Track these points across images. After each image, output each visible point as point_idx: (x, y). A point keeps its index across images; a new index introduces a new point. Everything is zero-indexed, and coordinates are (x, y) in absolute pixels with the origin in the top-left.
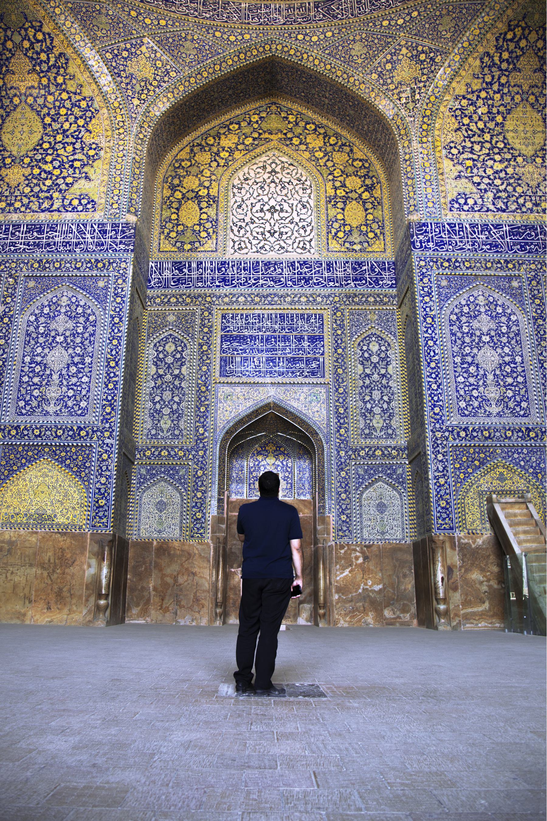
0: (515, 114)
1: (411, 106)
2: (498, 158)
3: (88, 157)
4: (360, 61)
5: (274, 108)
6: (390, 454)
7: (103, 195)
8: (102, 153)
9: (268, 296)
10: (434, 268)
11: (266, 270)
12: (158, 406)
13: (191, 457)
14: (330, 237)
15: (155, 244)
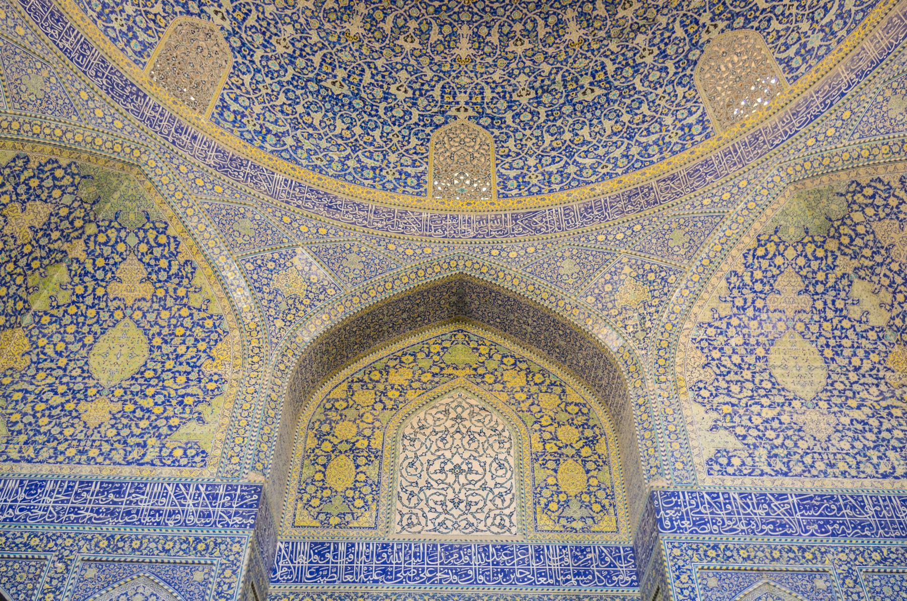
0: (780, 345)
1: (641, 335)
2: (765, 401)
3: (206, 392)
4: (571, 281)
5: (460, 336)
7: (219, 444)
8: (226, 387)
10: (695, 559)
11: (447, 558)
14: (539, 509)
15: (289, 516)
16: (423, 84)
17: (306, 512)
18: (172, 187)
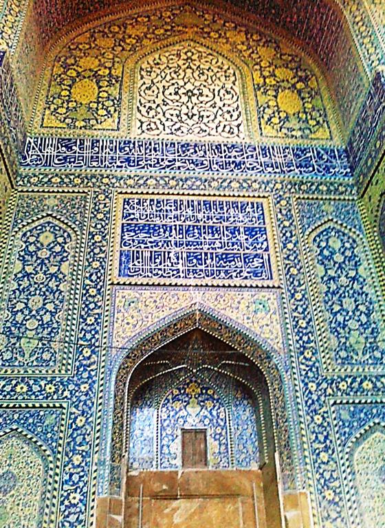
5: (187, 7)
9: (187, 179)
11: (184, 152)
12: (19, 317)
13: (66, 393)
15: (38, 119)
17: (53, 117)
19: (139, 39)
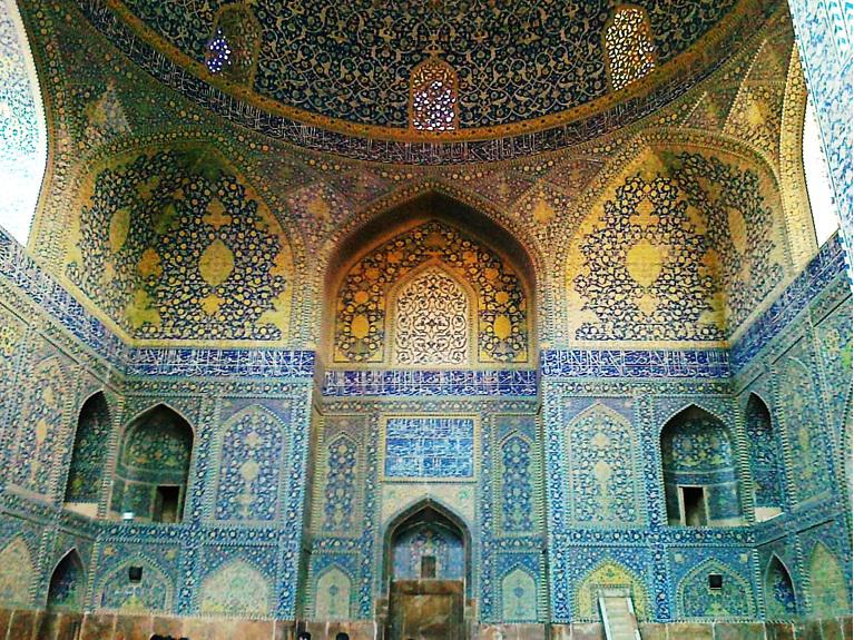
1: (547, 242)
2: (619, 289)
3: (274, 289)
4: (505, 200)
5: (435, 225)
6: (527, 544)
16: (403, 27)
18: (235, 153)
19: (397, 268)
